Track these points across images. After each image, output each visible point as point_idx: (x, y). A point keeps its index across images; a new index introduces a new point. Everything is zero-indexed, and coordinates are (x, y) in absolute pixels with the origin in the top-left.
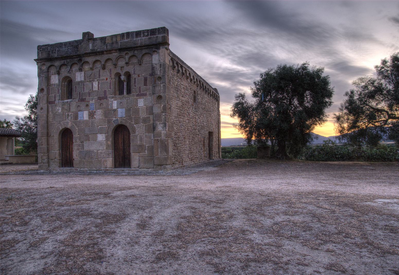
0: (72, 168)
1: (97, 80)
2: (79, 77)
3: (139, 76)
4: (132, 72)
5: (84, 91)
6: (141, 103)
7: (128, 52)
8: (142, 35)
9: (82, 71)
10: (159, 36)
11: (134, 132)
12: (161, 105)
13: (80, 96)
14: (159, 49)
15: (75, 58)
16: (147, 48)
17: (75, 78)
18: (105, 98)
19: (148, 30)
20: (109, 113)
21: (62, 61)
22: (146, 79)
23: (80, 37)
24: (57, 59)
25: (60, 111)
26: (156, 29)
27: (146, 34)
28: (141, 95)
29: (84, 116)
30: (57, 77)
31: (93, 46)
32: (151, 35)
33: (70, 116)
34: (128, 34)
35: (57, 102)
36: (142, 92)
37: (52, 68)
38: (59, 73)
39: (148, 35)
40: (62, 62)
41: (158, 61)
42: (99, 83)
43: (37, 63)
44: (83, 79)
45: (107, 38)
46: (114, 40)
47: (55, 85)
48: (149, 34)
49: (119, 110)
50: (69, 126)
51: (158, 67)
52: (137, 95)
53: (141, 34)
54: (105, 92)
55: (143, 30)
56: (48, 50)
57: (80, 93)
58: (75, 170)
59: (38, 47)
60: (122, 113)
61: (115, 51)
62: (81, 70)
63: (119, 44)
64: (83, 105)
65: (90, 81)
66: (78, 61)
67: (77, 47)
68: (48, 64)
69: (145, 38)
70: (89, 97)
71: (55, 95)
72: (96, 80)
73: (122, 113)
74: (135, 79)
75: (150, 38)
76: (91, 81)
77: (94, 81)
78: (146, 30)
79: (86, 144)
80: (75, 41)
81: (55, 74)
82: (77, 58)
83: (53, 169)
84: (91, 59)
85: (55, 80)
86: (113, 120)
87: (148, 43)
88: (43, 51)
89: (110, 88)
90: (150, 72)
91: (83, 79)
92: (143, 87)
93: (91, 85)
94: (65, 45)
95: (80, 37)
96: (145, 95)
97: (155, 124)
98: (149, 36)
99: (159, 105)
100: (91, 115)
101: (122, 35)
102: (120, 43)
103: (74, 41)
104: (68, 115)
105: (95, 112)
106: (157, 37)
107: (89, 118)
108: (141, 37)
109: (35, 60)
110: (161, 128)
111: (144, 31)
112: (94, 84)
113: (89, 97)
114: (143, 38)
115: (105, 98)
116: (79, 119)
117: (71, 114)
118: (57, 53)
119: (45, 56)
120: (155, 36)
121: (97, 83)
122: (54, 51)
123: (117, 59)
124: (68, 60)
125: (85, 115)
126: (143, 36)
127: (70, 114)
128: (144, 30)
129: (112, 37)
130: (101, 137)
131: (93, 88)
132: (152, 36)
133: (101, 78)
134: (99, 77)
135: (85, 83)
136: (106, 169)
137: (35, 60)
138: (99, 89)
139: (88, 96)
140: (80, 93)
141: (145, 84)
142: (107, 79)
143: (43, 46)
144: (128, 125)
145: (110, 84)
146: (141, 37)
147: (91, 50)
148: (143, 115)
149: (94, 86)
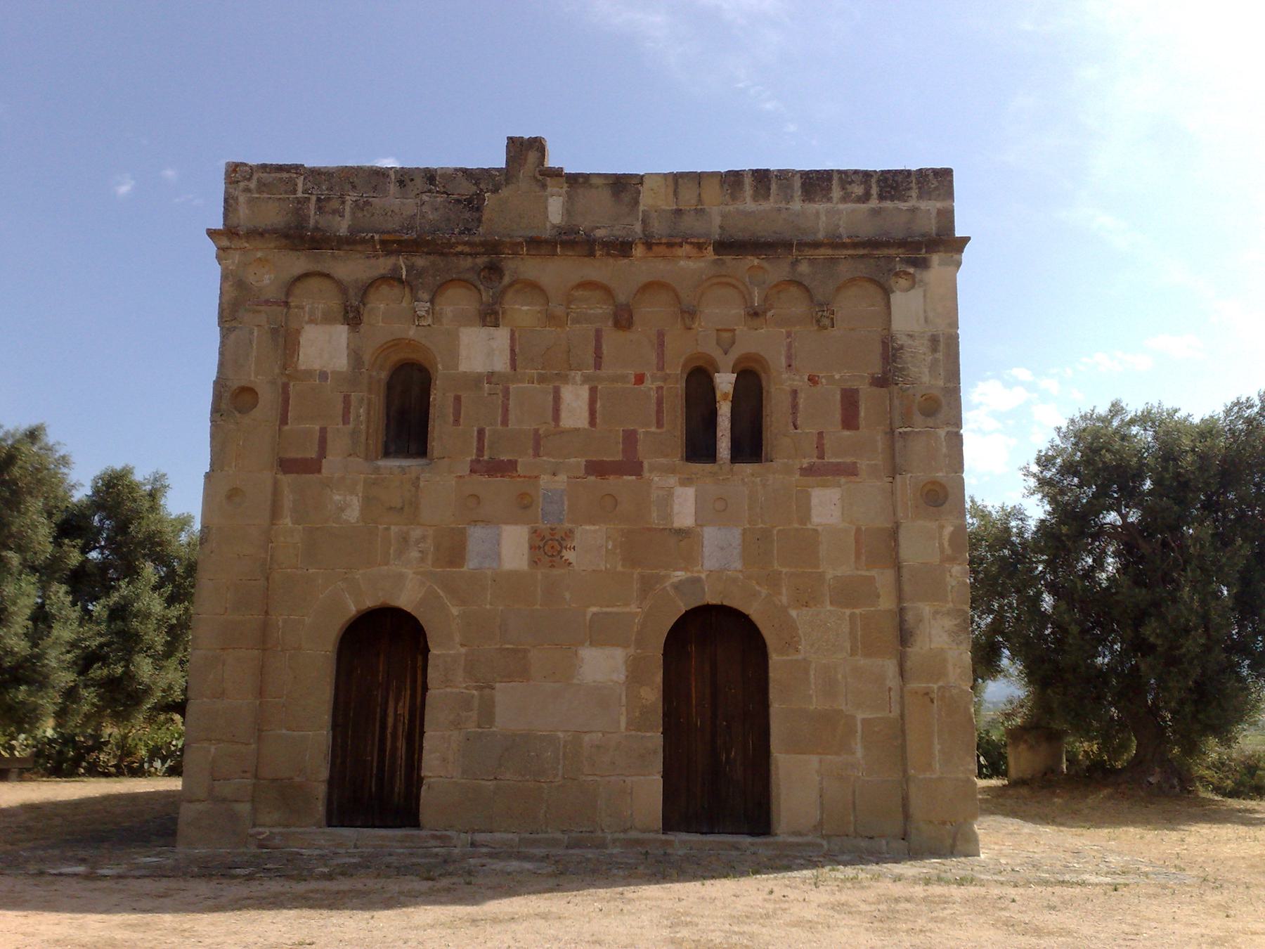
0: (414, 832)
1: (586, 379)
2: (479, 350)
3: (813, 380)
4: (777, 360)
5: (505, 422)
6: (827, 506)
7: (765, 265)
8: (836, 193)
9: (497, 326)
10: (924, 205)
11: (791, 644)
12: (942, 527)
13: (480, 450)
14: (923, 264)
15: (461, 253)
16: (863, 256)
17: (454, 354)
18: (632, 466)
19: (867, 175)
20: (651, 544)
21: (381, 260)
22: (850, 401)
23: (497, 160)
24: (350, 242)
25: (353, 514)
26: (908, 173)
27: (858, 190)
28: (820, 471)
29: (504, 551)
30: (341, 333)
31: (568, 211)
32: (881, 198)
33: (417, 542)
34: (762, 177)
35: (333, 464)
36: (830, 459)
37: (314, 283)
38: (352, 317)
39: (866, 197)
40: (384, 265)
41: (922, 320)
42: (593, 391)
43: (222, 249)
44: (501, 364)
45: (647, 182)
46: (688, 196)
47: (323, 375)
48: (875, 191)
49: (711, 536)
50: (406, 600)
51: (921, 347)
52: (808, 471)
53: (829, 189)
54: (630, 438)
55: (839, 172)
56: (295, 192)
57: (481, 432)
58: (433, 843)
59: (235, 171)
60: (722, 549)
61: (694, 252)
62: (490, 316)
63: (717, 221)
64: (497, 490)
65: (542, 379)
66: (479, 275)
67: (473, 204)
68: (298, 263)
69: (850, 206)
70: (537, 454)
71: (323, 431)
72: (578, 378)
73: (722, 549)
74: (795, 393)
75: (876, 212)
76: (554, 377)
77: (565, 379)
78: (856, 172)
79: (505, 696)
80: (465, 172)
81: (328, 319)
82: (474, 255)
83: (281, 834)
84: (555, 272)
85: (325, 347)
86: (675, 580)
87: (867, 230)
88: (259, 191)
89: (659, 424)
90: (877, 370)
91: (501, 364)
92: (837, 435)
93: (551, 398)
94: (401, 183)
95: (497, 160)
96: (850, 471)
97: (910, 617)
98: (874, 203)
99: (933, 525)
100: (548, 547)
101: (733, 180)
102: (718, 214)
103: (456, 170)
104: (405, 540)
105: (570, 534)
106: (913, 210)
107: (534, 563)
108: (830, 200)
109: (212, 233)
110: (945, 637)
111: (846, 177)
112: (567, 393)
113: (537, 454)
114: (841, 206)
115: (632, 466)
116: (471, 564)
117: (424, 538)
118: (353, 213)
119: (273, 214)
120: (903, 206)
121: (585, 392)
122: (335, 204)
123: (715, 280)
124: (420, 262)
125: (512, 547)
126: (845, 199)
127: (416, 533)
128: (845, 172)
129: (677, 180)
130: (603, 665)
131: (563, 415)
132: (888, 204)
133: (606, 371)
134: (598, 366)
135: (512, 387)
136: (622, 836)
137: (212, 233)
138: (592, 422)
139: (531, 451)
140: (481, 432)
141: (850, 421)
142: (640, 379)
143: (264, 167)
144: (754, 610)
145: (660, 403)
146: (830, 200)
147: (554, 226)
148: (837, 567)
149: (563, 407)
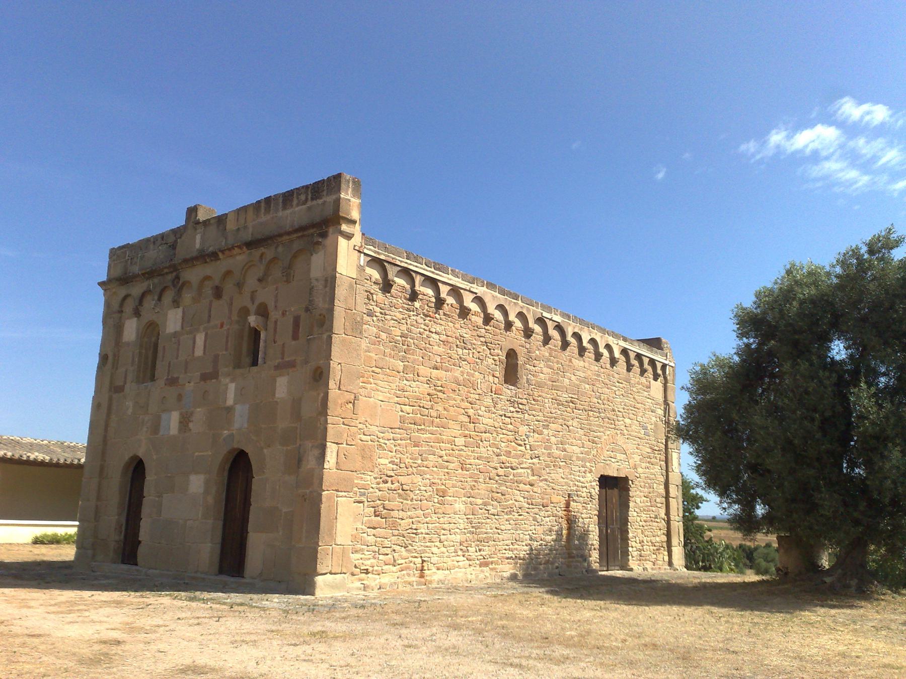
8: (295, 202)
12: (319, 394)
14: (324, 235)
19: (307, 187)
27: (303, 197)
28: (285, 366)
32: (312, 199)
38: (137, 313)
44: (178, 328)
48: (309, 197)
49: (238, 408)
52: (277, 367)
62: (176, 303)
74: (276, 322)
75: (309, 208)
82: (172, 272)
91: (178, 328)
98: (309, 203)
100: (184, 422)
105: (192, 414)
109: (101, 284)
112: (198, 339)
116: (161, 433)
122: (135, 260)
126: (298, 205)
129: (239, 211)
130: (196, 483)
132: (315, 202)
134: (209, 321)
137: (101, 284)
142: (222, 326)
